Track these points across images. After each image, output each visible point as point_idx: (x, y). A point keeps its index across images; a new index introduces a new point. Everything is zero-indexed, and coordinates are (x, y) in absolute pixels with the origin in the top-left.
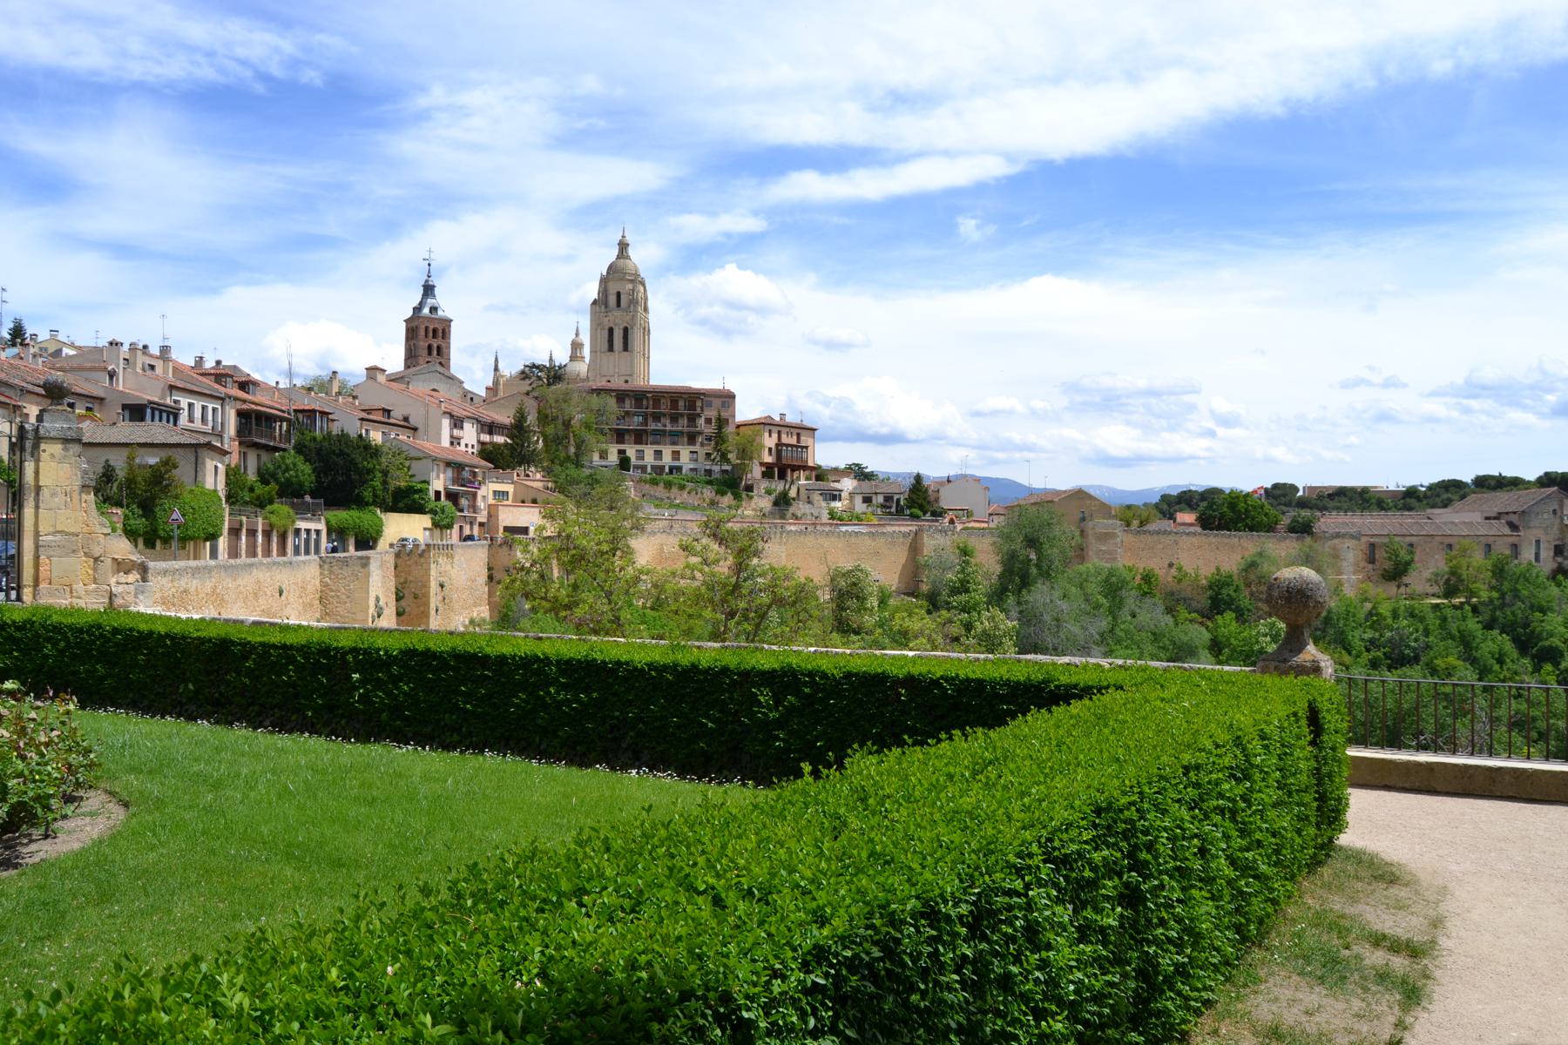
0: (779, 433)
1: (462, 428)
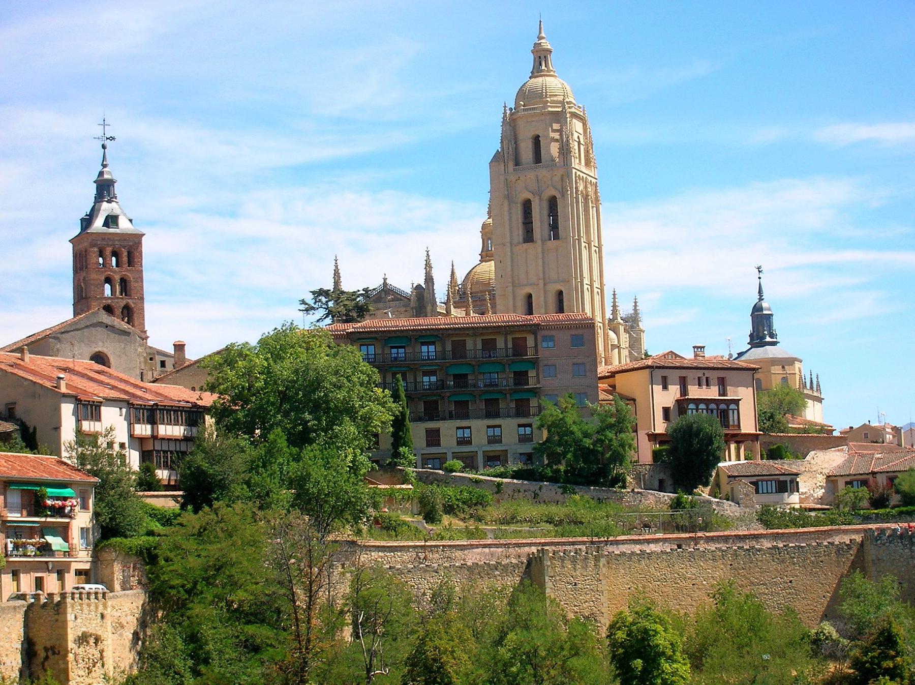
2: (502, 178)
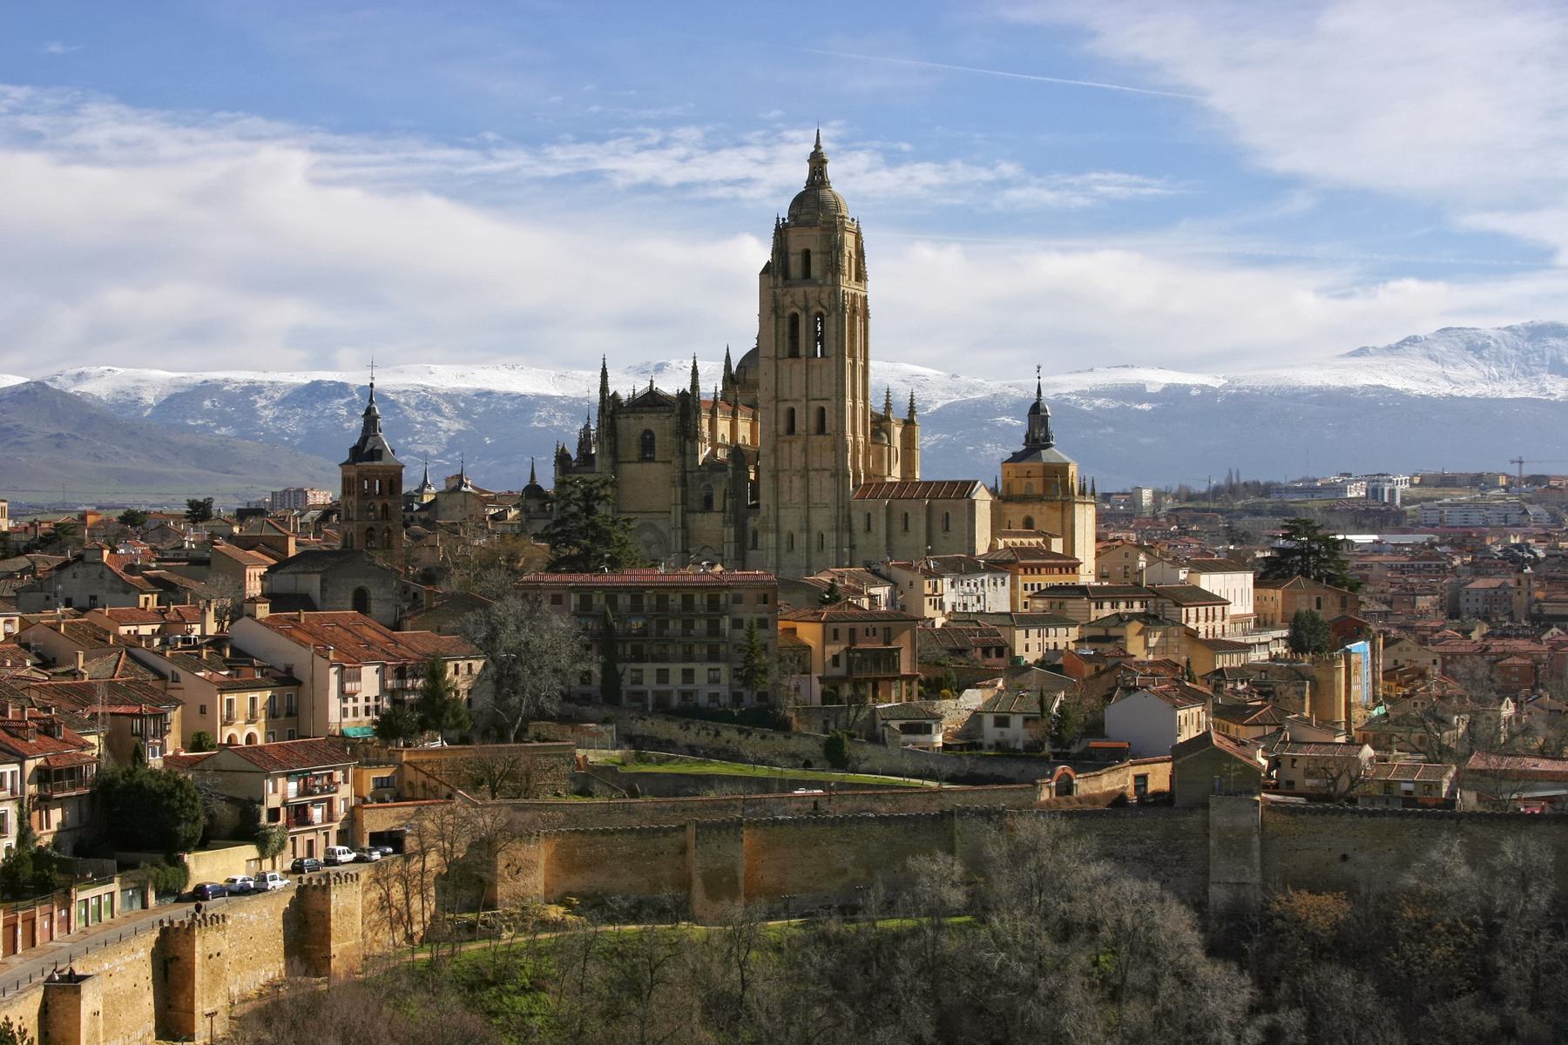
0: (852, 632)
1: (359, 679)
2: (771, 291)
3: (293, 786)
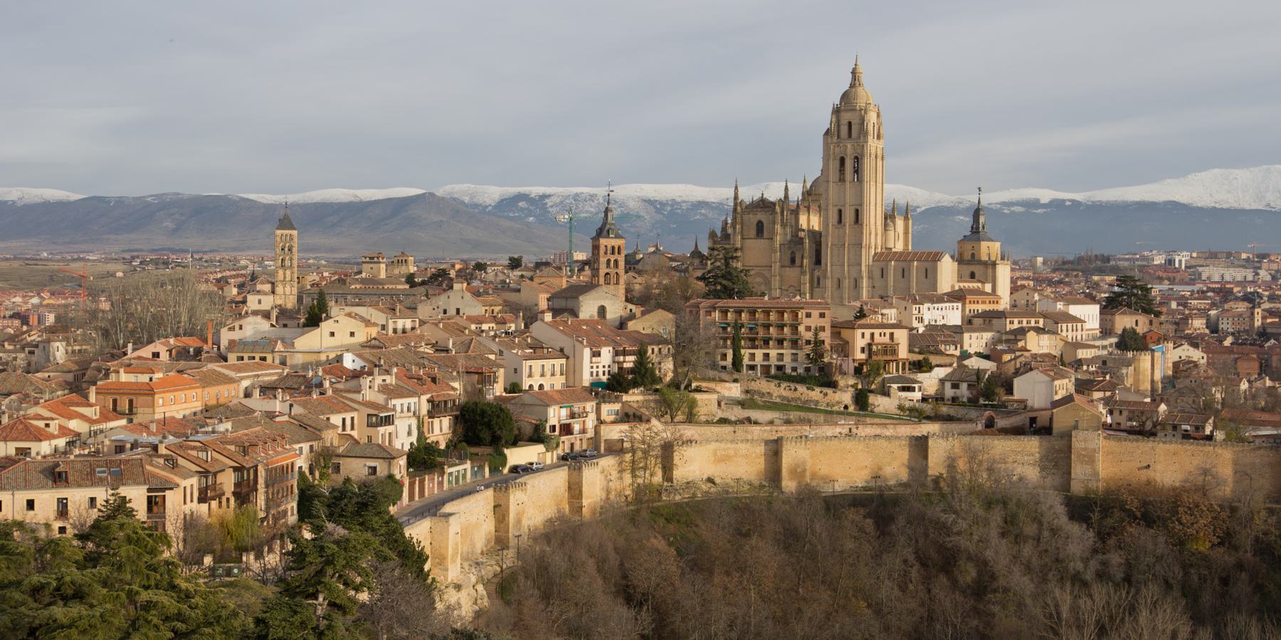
0: (872, 335)
3: (564, 412)
